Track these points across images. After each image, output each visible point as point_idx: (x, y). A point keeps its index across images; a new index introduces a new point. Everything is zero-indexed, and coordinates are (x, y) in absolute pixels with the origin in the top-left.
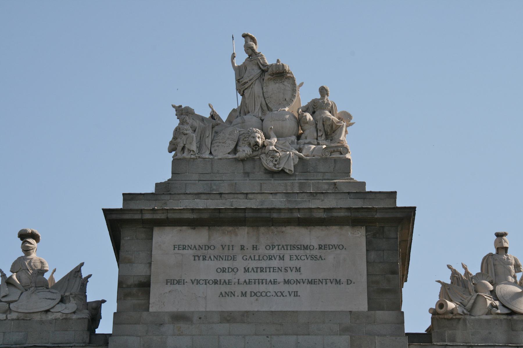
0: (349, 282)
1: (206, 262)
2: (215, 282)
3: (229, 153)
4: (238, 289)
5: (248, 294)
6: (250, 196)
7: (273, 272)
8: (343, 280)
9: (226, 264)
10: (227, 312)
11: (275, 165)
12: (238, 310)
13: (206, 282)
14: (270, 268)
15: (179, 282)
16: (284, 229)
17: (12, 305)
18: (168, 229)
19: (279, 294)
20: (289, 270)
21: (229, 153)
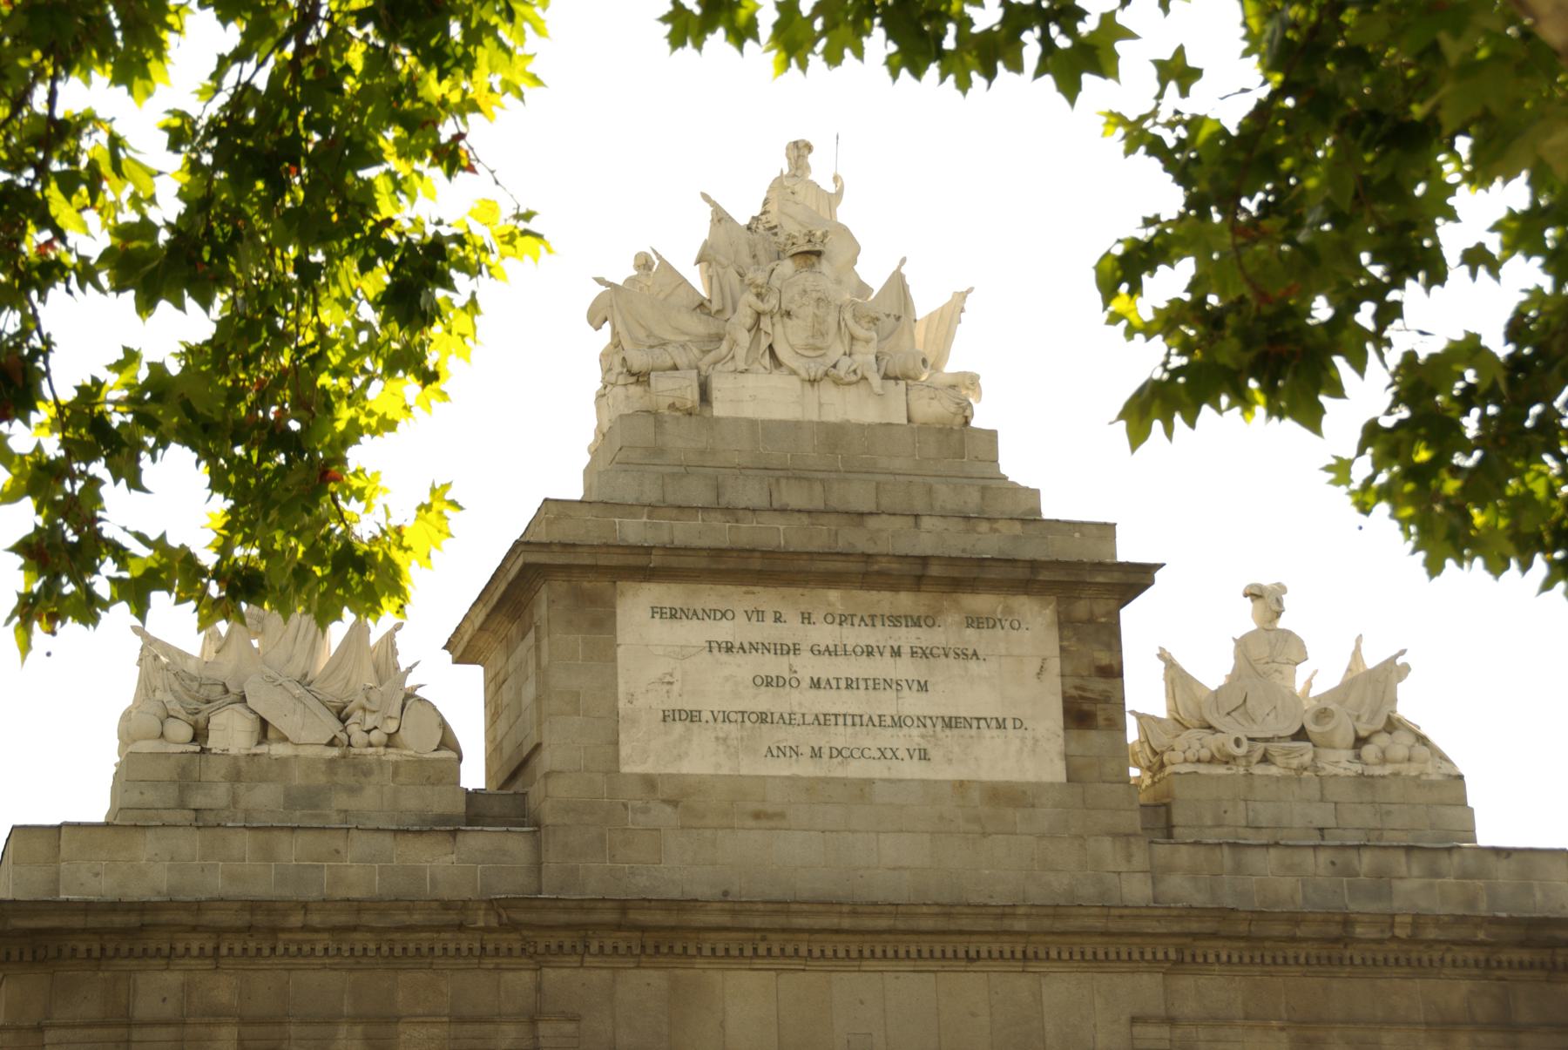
7: (875, 688)
9: (774, 665)
14: (866, 680)
20: (904, 684)
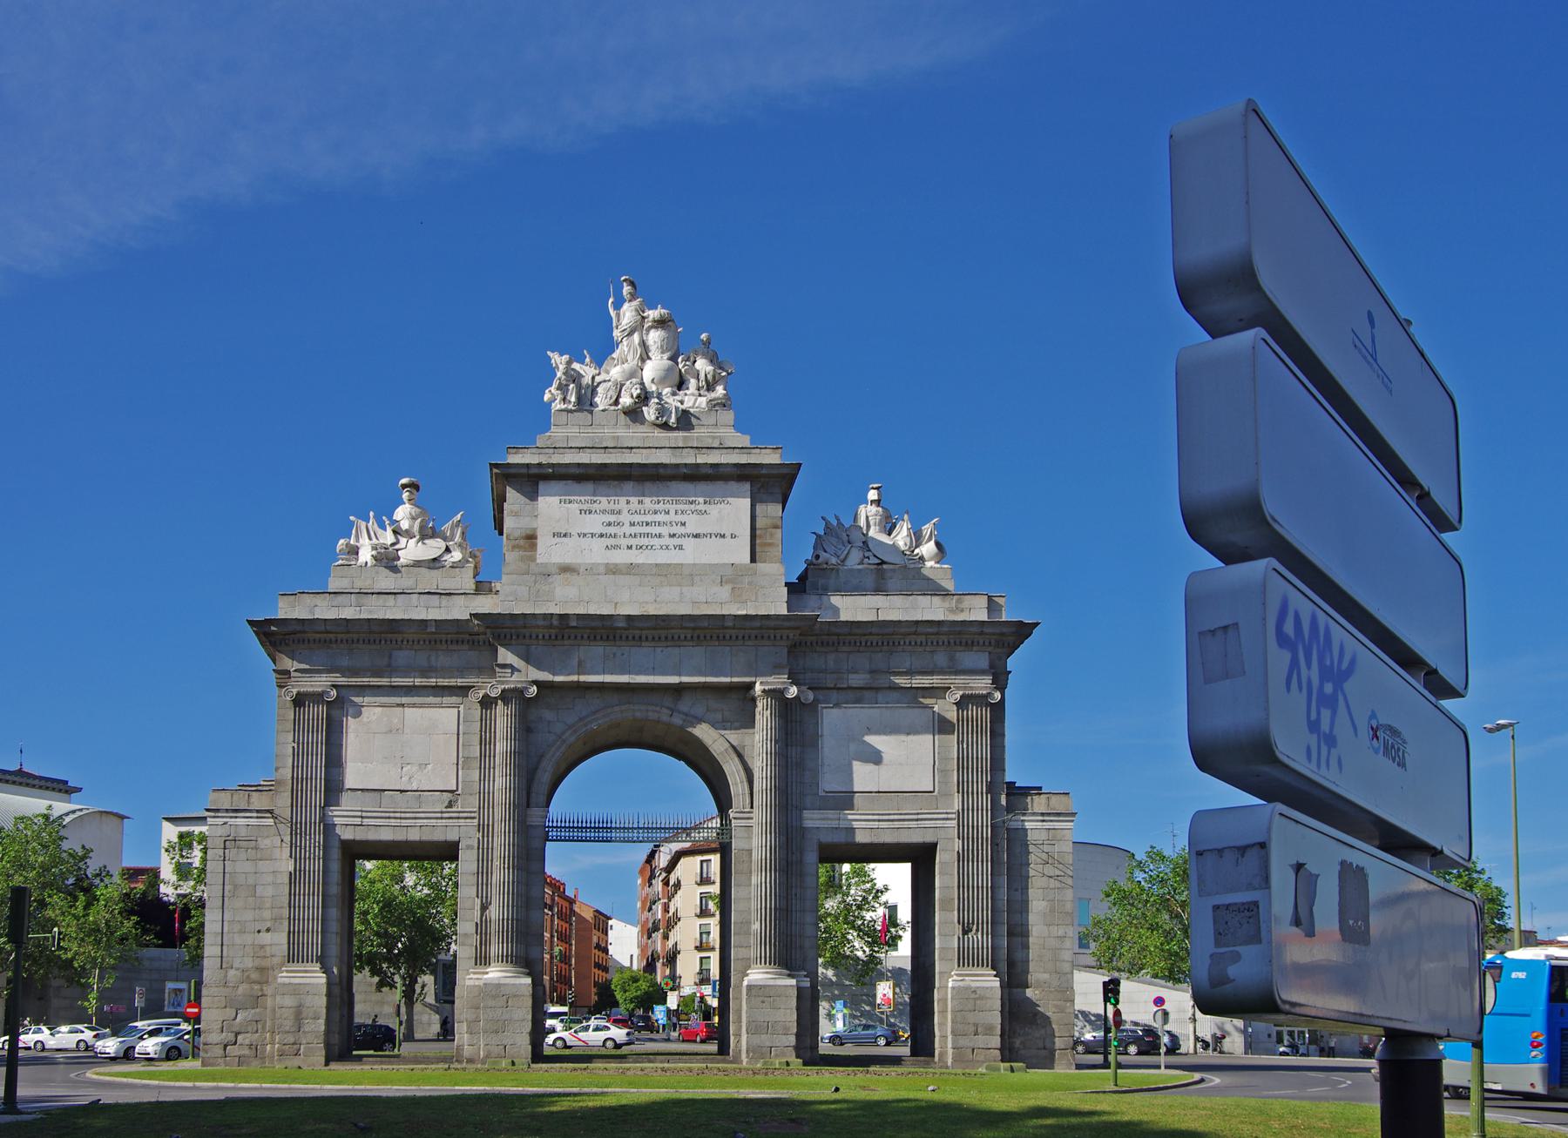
0: (733, 536)
1: (591, 515)
2: (601, 536)
3: (610, 405)
4: (624, 542)
5: (634, 547)
6: (634, 450)
8: (728, 535)
9: (612, 518)
10: (613, 564)
11: (657, 418)
12: (623, 562)
13: (593, 535)
15: (565, 535)
16: (669, 483)
17: (399, 552)
18: (553, 483)
19: (664, 547)
21: (610, 405)
